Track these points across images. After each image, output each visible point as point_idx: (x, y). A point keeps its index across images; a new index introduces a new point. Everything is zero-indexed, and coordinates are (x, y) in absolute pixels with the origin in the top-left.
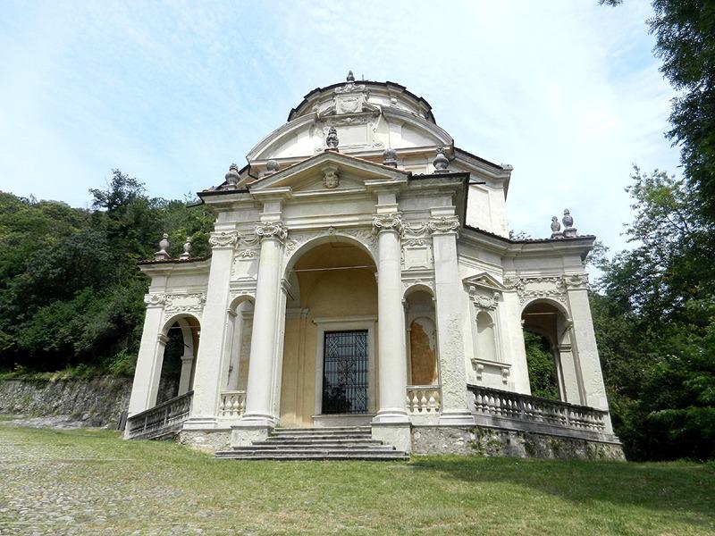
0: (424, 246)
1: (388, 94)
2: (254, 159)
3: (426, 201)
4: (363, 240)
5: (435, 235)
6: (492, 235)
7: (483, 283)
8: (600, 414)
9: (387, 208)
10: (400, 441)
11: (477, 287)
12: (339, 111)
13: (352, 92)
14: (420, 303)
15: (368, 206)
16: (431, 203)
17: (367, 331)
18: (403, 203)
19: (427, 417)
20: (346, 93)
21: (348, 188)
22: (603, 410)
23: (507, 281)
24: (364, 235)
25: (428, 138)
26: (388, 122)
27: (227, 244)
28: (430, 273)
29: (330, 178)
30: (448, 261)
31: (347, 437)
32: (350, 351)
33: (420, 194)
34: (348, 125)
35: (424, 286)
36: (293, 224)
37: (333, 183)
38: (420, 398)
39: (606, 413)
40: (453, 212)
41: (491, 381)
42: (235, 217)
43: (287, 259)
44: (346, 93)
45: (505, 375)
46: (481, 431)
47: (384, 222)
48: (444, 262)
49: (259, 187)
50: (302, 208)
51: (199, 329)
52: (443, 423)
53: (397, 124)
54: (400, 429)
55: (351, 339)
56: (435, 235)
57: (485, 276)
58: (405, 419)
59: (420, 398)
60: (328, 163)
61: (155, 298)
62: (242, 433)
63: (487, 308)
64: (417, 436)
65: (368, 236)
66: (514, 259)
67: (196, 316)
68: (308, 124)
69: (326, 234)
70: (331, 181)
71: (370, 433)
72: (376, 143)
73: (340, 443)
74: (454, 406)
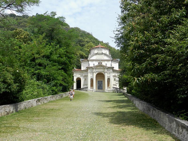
9: (106, 70)
10: (107, 91)
12: (99, 53)
14: (109, 79)
16: (110, 70)
19: (109, 89)
21: (102, 68)
32: (101, 83)
33: (109, 69)
34: (100, 55)
36: (96, 71)
41: (115, 86)
42: (90, 70)
46: (113, 91)
55: (101, 82)
57: (115, 75)
61: (75, 75)
74: (112, 89)
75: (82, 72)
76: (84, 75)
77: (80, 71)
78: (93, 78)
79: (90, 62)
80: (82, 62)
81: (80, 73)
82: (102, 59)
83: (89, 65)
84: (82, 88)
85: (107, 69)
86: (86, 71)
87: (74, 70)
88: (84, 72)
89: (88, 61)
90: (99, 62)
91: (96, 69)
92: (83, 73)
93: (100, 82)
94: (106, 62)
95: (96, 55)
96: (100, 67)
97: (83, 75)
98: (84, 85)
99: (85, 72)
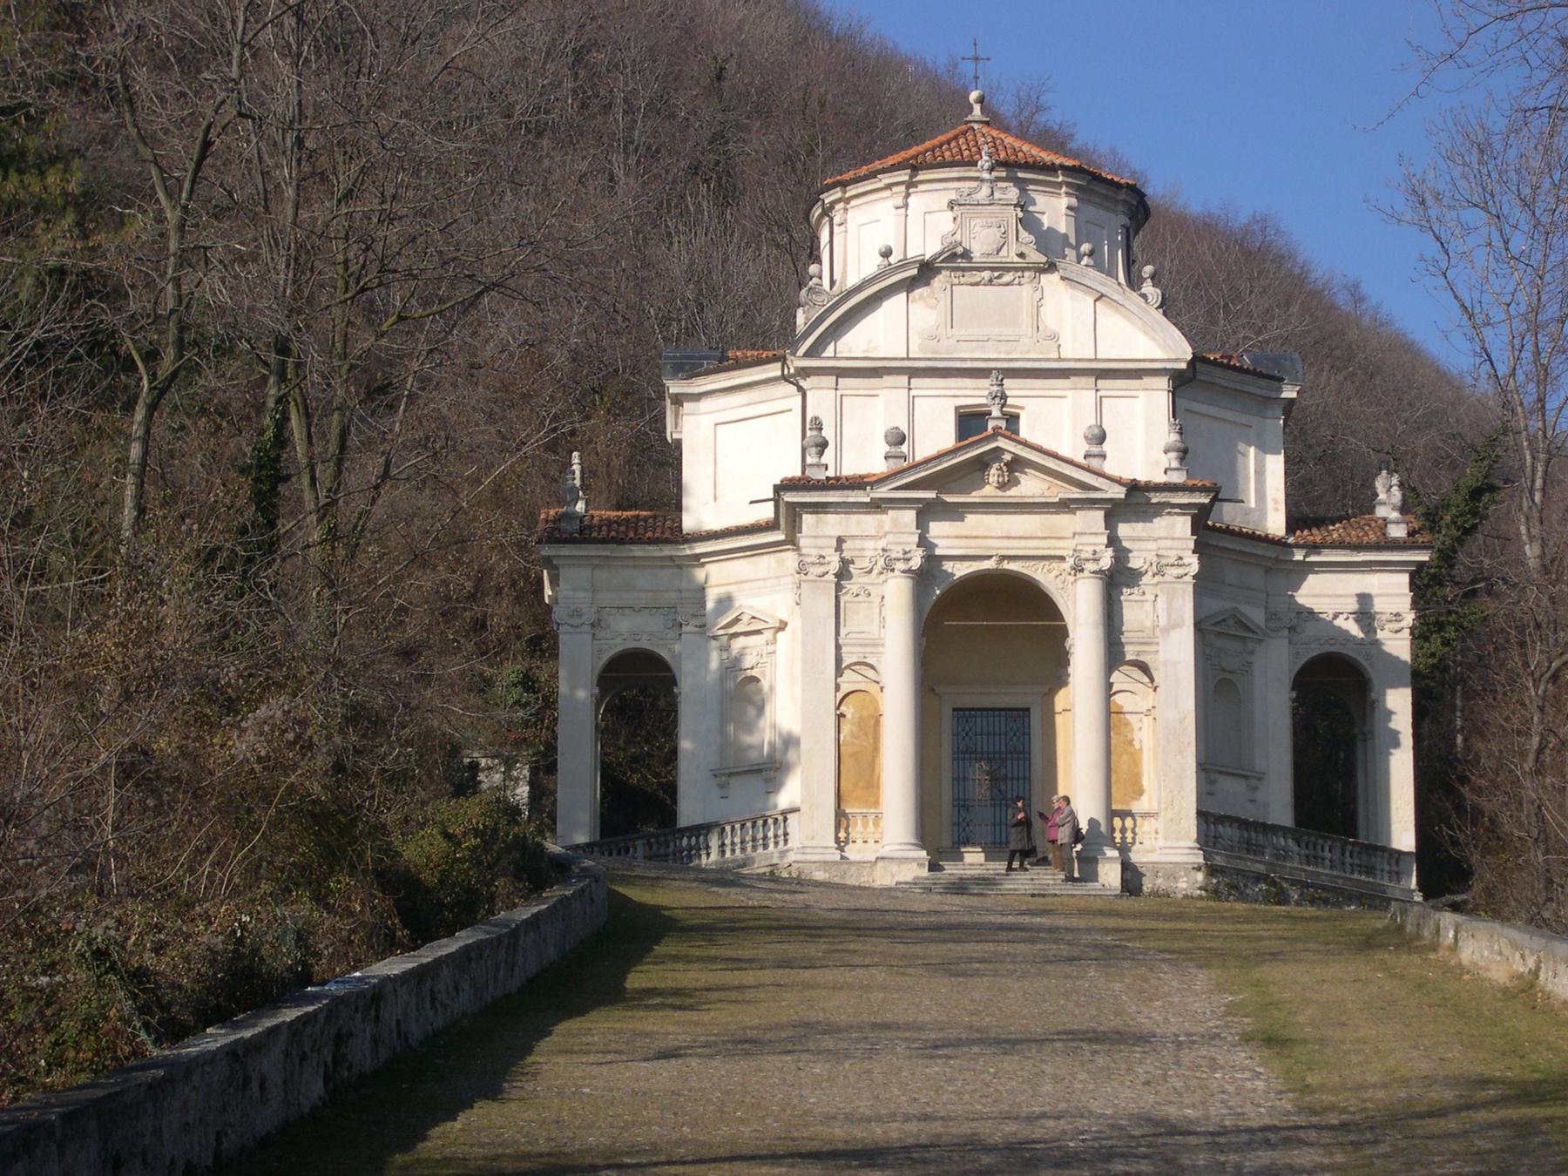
51: (673, 681)
65: (1055, 573)
82: (1029, 352)
90: (975, 394)
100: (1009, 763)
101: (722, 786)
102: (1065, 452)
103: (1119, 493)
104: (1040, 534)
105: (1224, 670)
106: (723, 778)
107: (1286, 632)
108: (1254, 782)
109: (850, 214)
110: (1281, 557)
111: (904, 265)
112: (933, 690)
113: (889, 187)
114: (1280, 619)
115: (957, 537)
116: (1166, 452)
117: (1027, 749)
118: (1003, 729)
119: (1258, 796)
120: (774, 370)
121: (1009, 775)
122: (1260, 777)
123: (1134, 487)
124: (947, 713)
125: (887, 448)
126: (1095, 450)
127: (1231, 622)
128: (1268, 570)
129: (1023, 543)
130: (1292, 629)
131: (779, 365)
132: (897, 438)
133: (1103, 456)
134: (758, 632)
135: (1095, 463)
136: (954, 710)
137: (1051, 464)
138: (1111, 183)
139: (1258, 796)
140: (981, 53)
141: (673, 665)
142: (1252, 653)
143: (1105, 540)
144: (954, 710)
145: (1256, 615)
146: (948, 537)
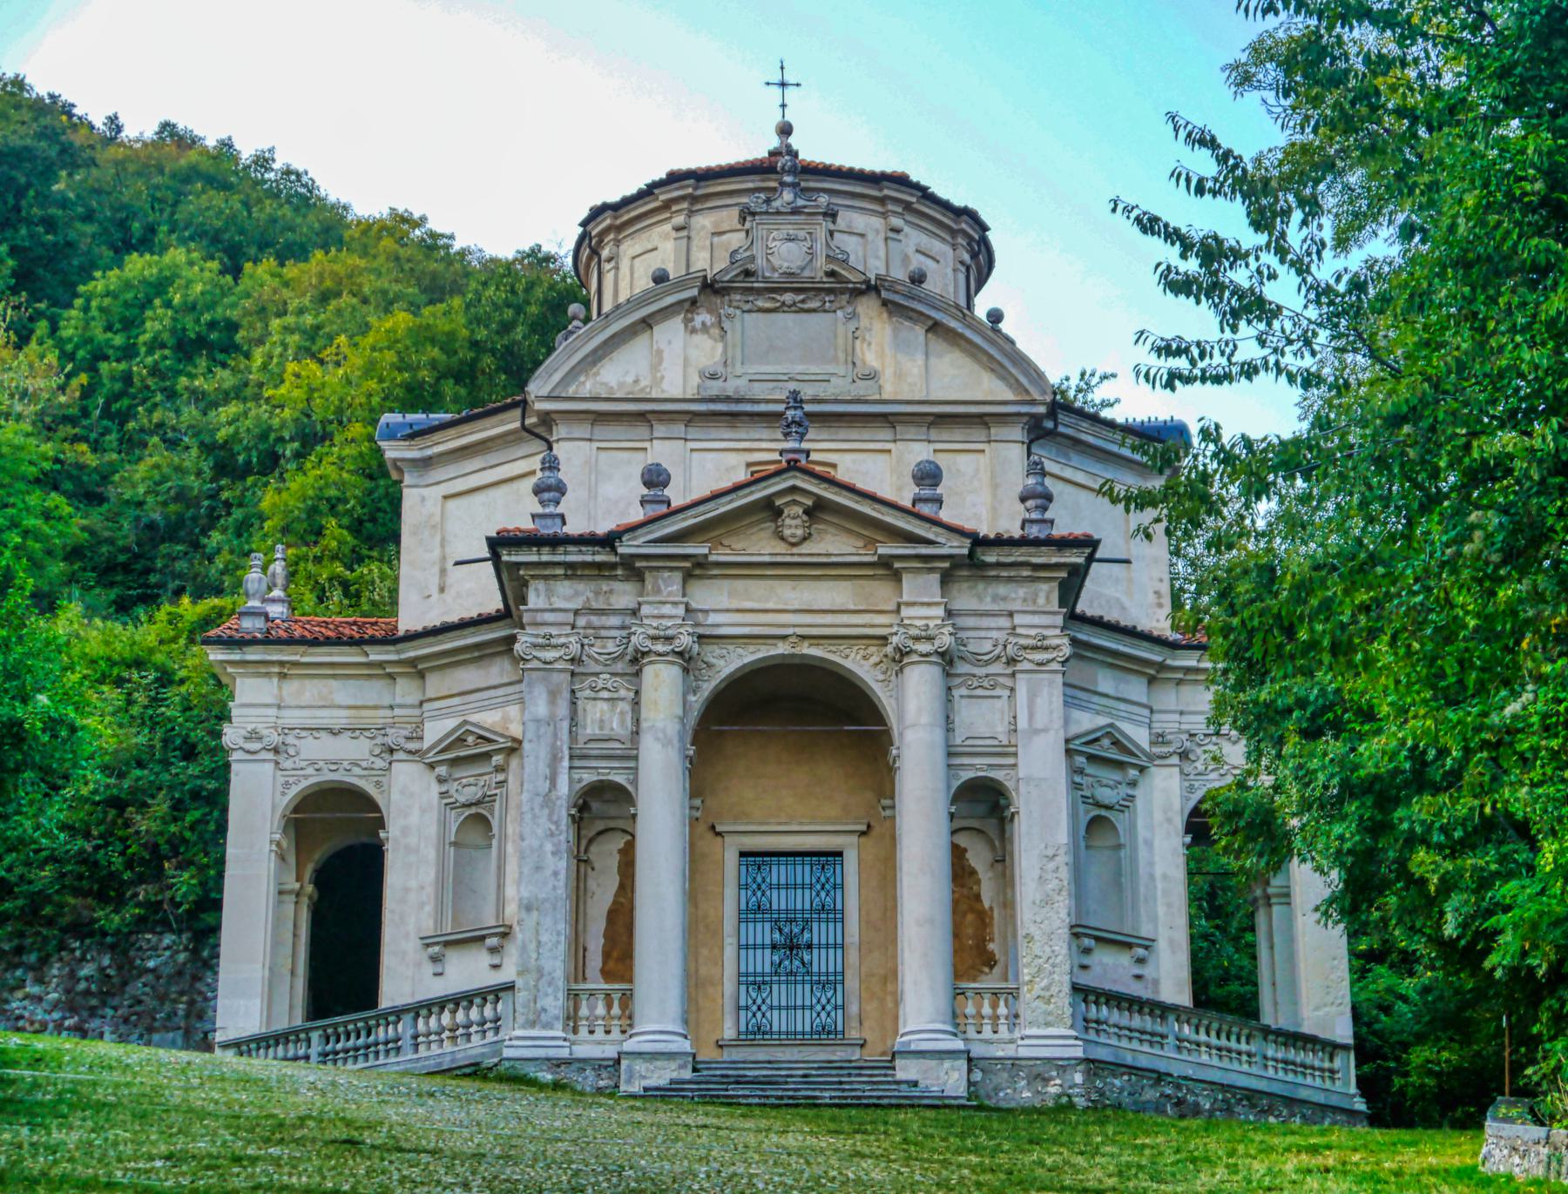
0: (997, 692)
1: (882, 201)
2: (544, 392)
3: (1002, 589)
4: (862, 666)
5: (1022, 672)
6: (1131, 633)
7: (1106, 749)
8: (1332, 1048)
10: (951, 1080)
11: (1092, 758)
13: (796, 211)
15: (881, 593)
17: (840, 854)
18: (955, 588)
20: (778, 213)
21: (833, 544)
22: (1339, 1040)
23: (1159, 739)
24: (864, 658)
25: (992, 370)
26: (890, 313)
27: (556, 660)
28: (1007, 752)
29: (793, 522)
30: (1045, 730)
31: (849, 1075)
32: (802, 900)
35: (992, 780)
37: (799, 532)
38: (994, 1006)
39: (1345, 1047)
40: (1059, 620)
41: (1112, 969)
43: (698, 701)
44: (778, 213)
45: (1141, 961)
47: (917, 639)
48: (1037, 732)
49: (634, 538)
50: (726, 584)
51: (380, 823)
52: (1023, 1052)
53: (915, 322)
54: (947, 1064)
55: (803, 872)
56: (1022, 672)
58: (959, 1045)
59: (994, 1006)
60: (794, 489)
61: (254, 736)
62: (640, 1066)
63: (1108, 808)
64: (977, 1076)
65: (874, 659)
66: (1179, 682)
67: (368, 787)
68: (680, 302)
69: (782, 649)
70: (793, 525)
71: (893, 1068)
72: (860, 370)
73: (841, 1083)
75: (417, 670)
76: (451, 723)
77: (376, 653)
78: (635, 782)
79: (573, 453)
80: (426, 463)
81: (373, 692)
82: (838, 387)
83: (550, 491)
84: (399, 1013)
85: (946, 579)
86: (481, 654)
87: (250, 625)
88: (454, 659)
89: (541, 430)
91: (696, 570)
92: (437, 684)
93: (779, 873)
94: (918, 452)
95: (702, 317)
96: (793, 525)
97: (434, 731)
98: (444, 945)
99: (469, 677)
100: (815, 925)
101: (435, 959)
102: (887, 493)
103: (960, 547)
104: (852, 607)
105: (1098, 805)
106: (436, 949)
107: (1175, 760)
108: (1140, 952)
109: (623, 247)
110: (1169, 662)
111: (682, 284)
112: (713, 827)
113: (667, 205)
114: (1169, 743)
115: (738, 611)
116: (1023, 499)
117: (839, 906)
118: (807, 881)
119: (1147, 971)
120: (510, 423)
121: (815, 941)
122: (1148, 944)
123: (978, 542)
124: (731, 859)
125: (645, 491)
126: (927, 492)
127: (1106, 742)
128: (1152, 680)
129: (829, 619)
130: (1184, 755)
131: (518, 412)
132: (655, 478)
133: (939, 501)
134: (487, 756)
135: (926, 509)
136: (743, 854)
137: (866, 508)
138: (946, 206)
139: (1147, 971)
140: (789, 78)
141: (380, 800)
142: (1133, 784)
143: (939, 611)
144: (743, 854)
145: (1140, 736)
146: (728, 611)
